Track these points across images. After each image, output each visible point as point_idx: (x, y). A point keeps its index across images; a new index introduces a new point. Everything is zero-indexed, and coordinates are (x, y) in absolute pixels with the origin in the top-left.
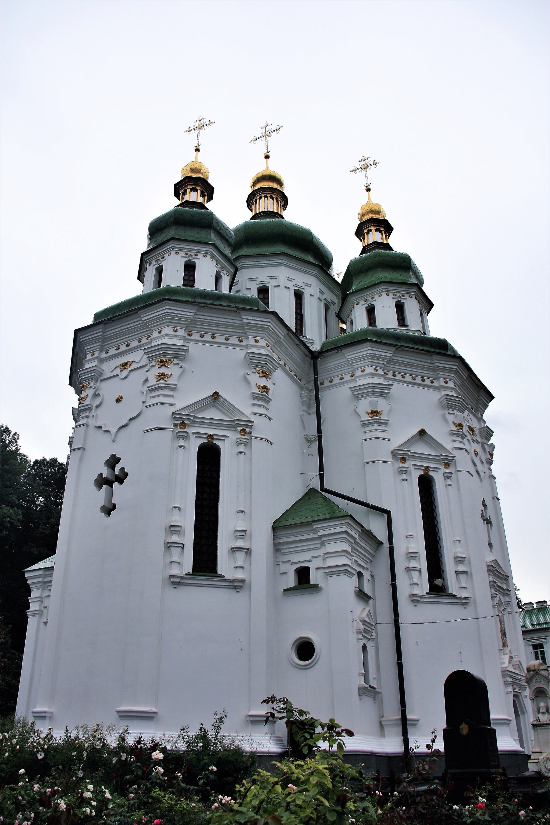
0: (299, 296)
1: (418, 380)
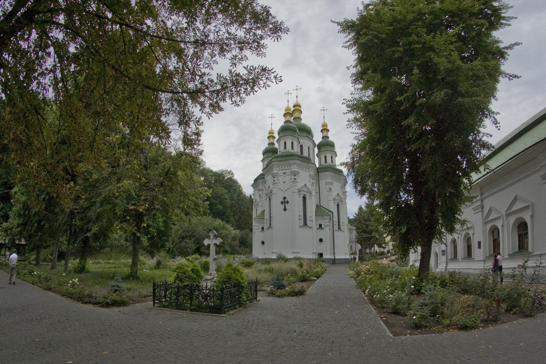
0: (309, 148)
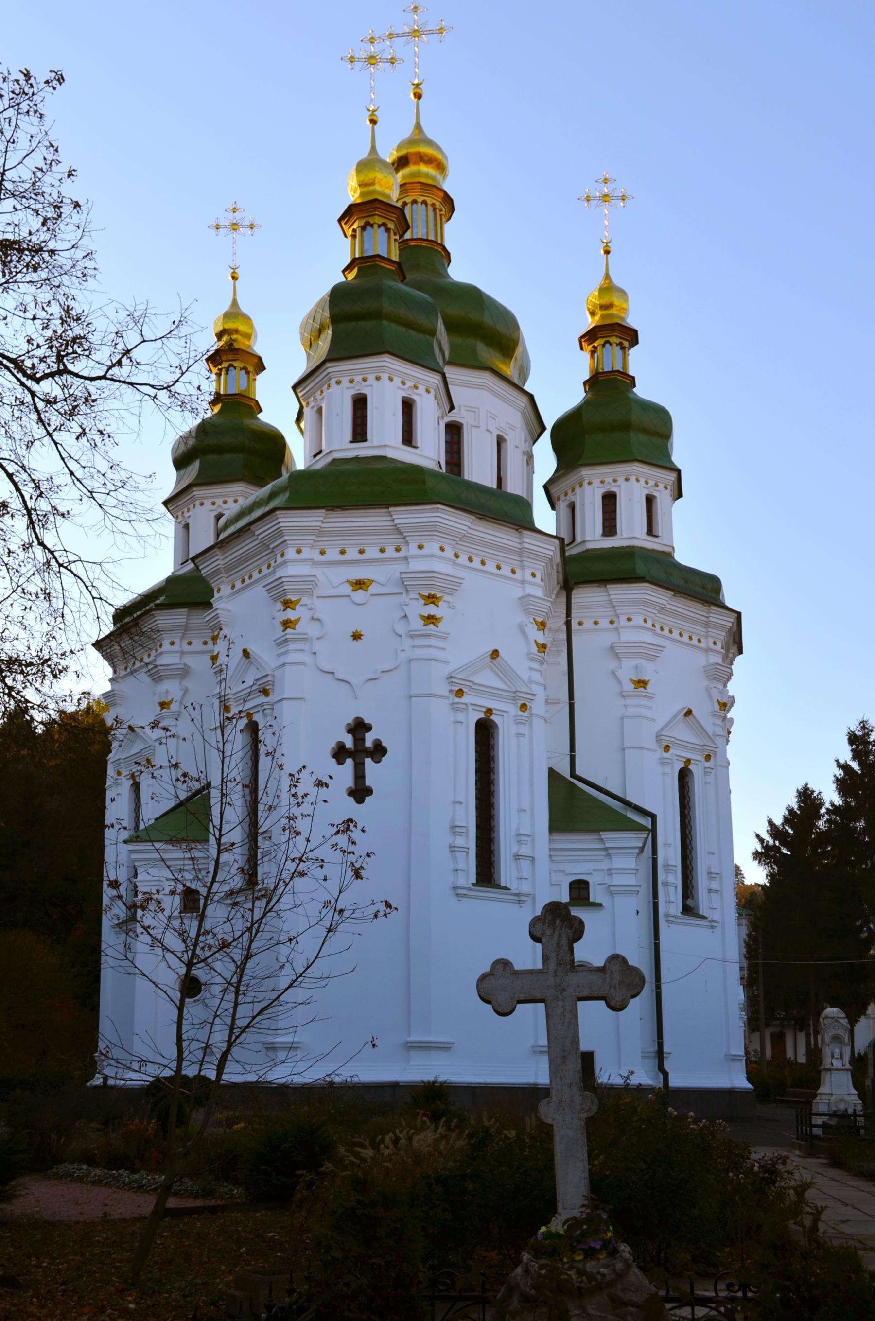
1: (685, 638)
